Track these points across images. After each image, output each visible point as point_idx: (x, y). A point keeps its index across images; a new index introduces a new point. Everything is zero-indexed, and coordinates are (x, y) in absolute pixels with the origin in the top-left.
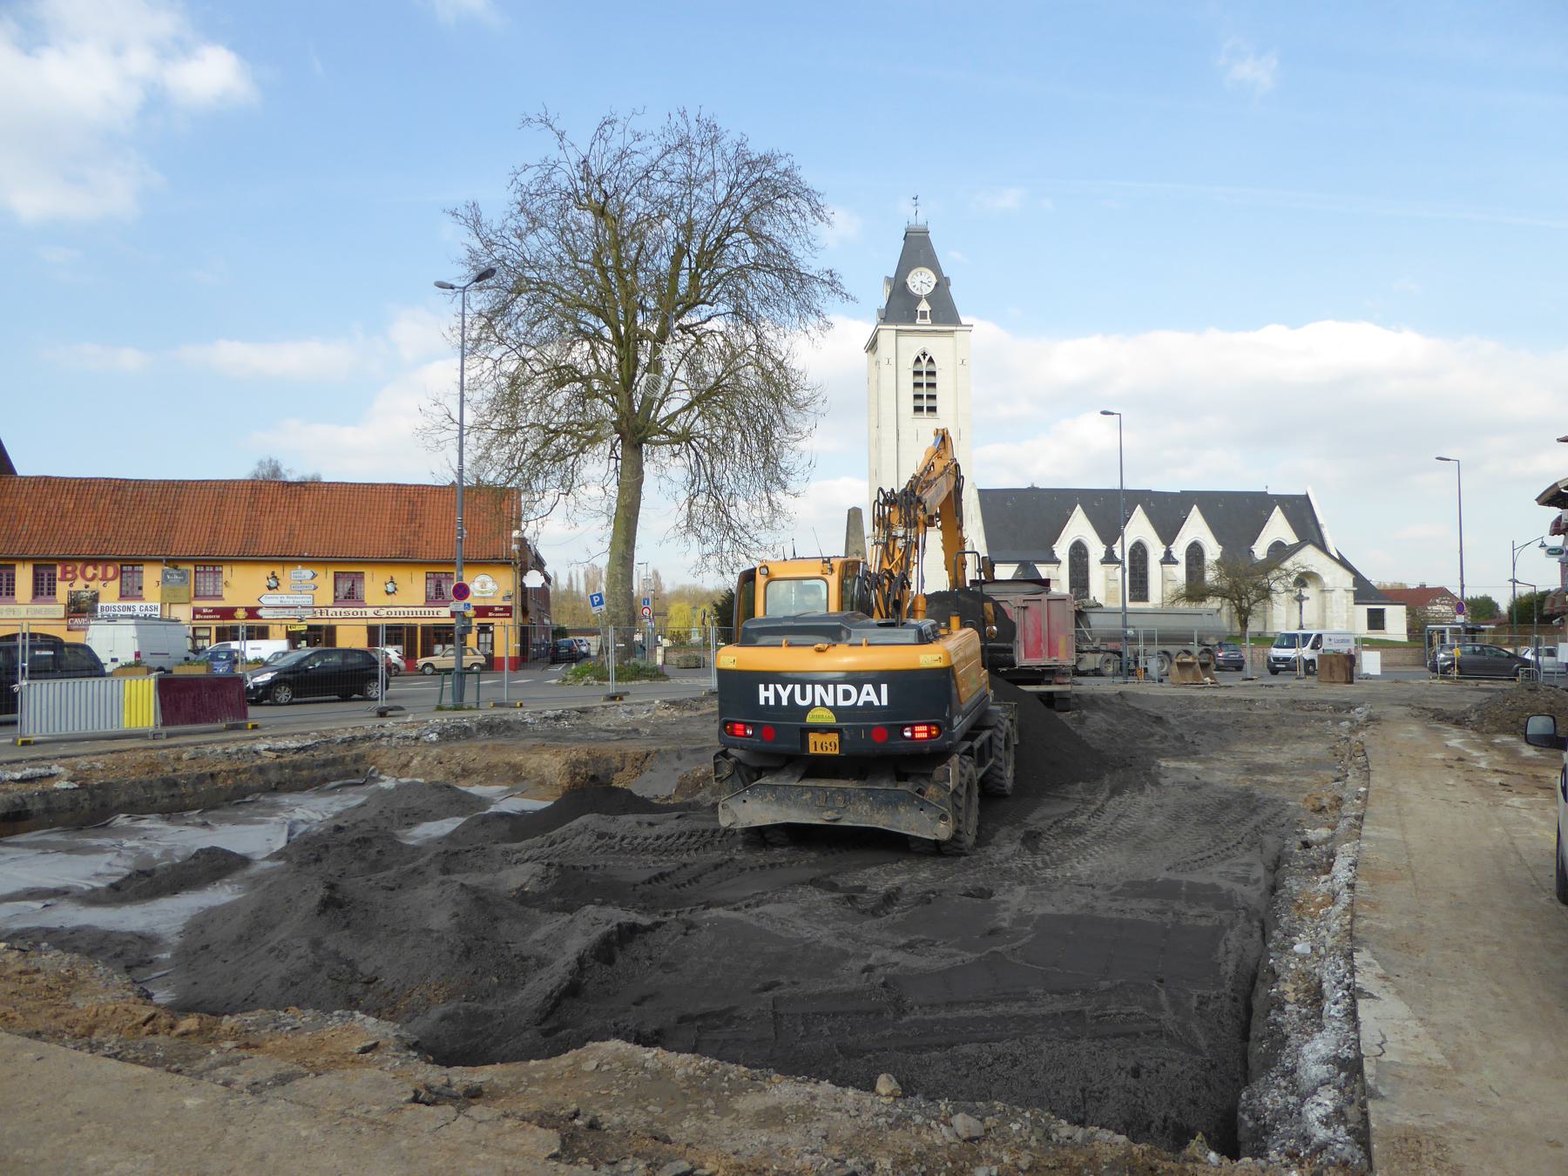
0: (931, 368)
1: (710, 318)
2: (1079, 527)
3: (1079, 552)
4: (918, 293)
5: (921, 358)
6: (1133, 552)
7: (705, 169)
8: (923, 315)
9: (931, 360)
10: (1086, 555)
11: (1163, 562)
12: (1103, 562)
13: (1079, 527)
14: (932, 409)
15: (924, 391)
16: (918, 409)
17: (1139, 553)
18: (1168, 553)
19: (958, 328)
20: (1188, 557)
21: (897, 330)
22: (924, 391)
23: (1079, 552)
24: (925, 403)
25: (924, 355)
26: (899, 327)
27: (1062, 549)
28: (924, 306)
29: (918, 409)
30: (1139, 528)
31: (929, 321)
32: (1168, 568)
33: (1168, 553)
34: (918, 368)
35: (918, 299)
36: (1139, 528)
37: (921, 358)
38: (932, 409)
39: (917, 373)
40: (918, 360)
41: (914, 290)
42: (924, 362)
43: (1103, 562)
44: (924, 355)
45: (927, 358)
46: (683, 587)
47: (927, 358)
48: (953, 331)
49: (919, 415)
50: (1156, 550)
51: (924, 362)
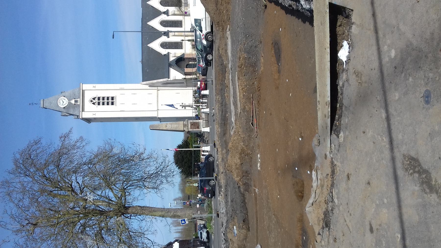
0: (96, 99)
1: (78, 183)
2: (155, 45)
3: (164, 45)
4: (67, 103)
5: (93, 102)
6: (165, 26)
7: (19, 186)
8: (76, 101)
9: (94, 99)
10: (166, 43)
11: (168, 15)
12: (168, 37)
13: (155, 45)
14: (113, 98)
15: (106, 101)
16: (112, 104)
17: (164, 23)
18: (164, 13)
19: (81, 88)
20: (166, 6)
21: (82, 112)
23: (164, 45)
25: (92, 101)
26: (81, 110)
27: (164, 51)
28: (73, 102)
29: (112, 104)
30: (155, 23)
32: (170, 13)
33: (164, 13)
34: (97, 104)
35: (70, 104)
36: (155, 23)
37: (93, 102)
38: (113, 98)
39: (99, 104)
40: (94, 104)
41: (66, 105)
42: (94, 101)
43: (168, 37)
45: (93, 100)
46: (180, 189)
47: (93, 100)
48: (82, 90)
49: (114, 103)
50: (163, 17)
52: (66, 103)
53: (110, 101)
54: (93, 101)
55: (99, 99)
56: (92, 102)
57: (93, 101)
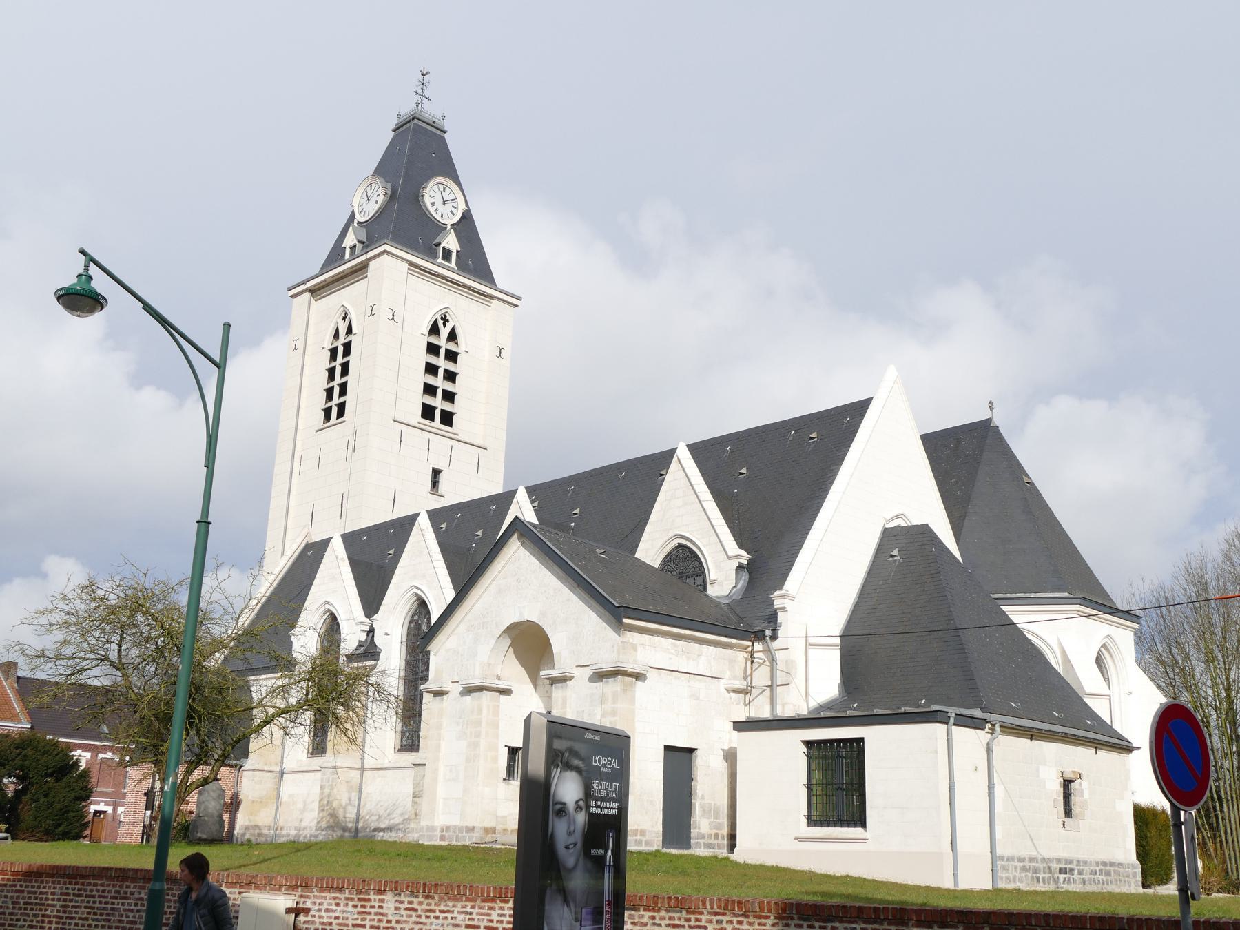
5: (440, 323)
8: (447, 254)
9: (452, 337)
14: (447, 418)
22: (439, 382)
24: (438, 403)
29: (428, 412)
31: (453, 265)
34: (434, 340)
37: (440, 323)
39: (433, 349)
42: (445, 332)
44: (445, 320)
45: (449, 326)
47: (449, 326)
51: (445, 332)
52: (439, 213)
53: (438, 403)
54: (445, 325)
55: (452, 356)
56: (442, 319)
57: (445, 325)
